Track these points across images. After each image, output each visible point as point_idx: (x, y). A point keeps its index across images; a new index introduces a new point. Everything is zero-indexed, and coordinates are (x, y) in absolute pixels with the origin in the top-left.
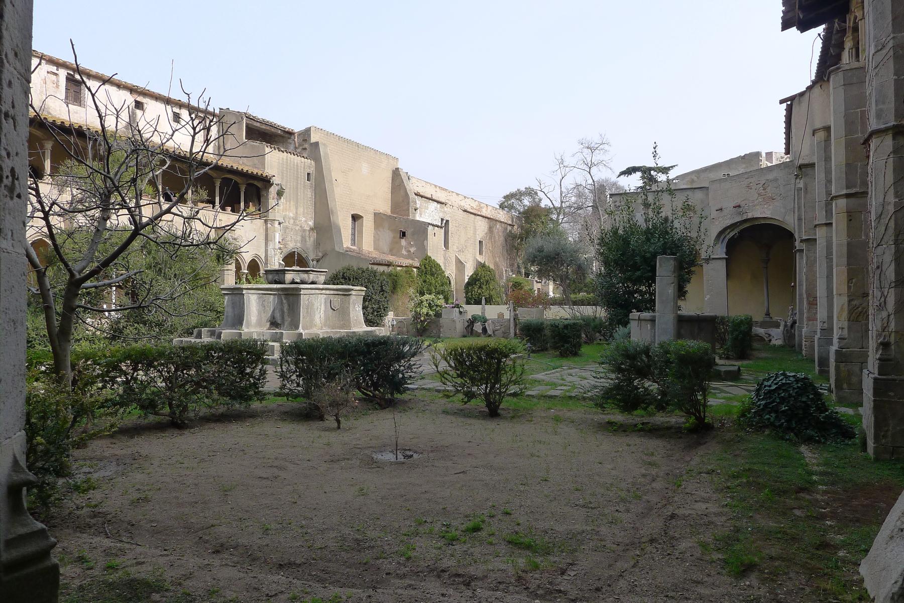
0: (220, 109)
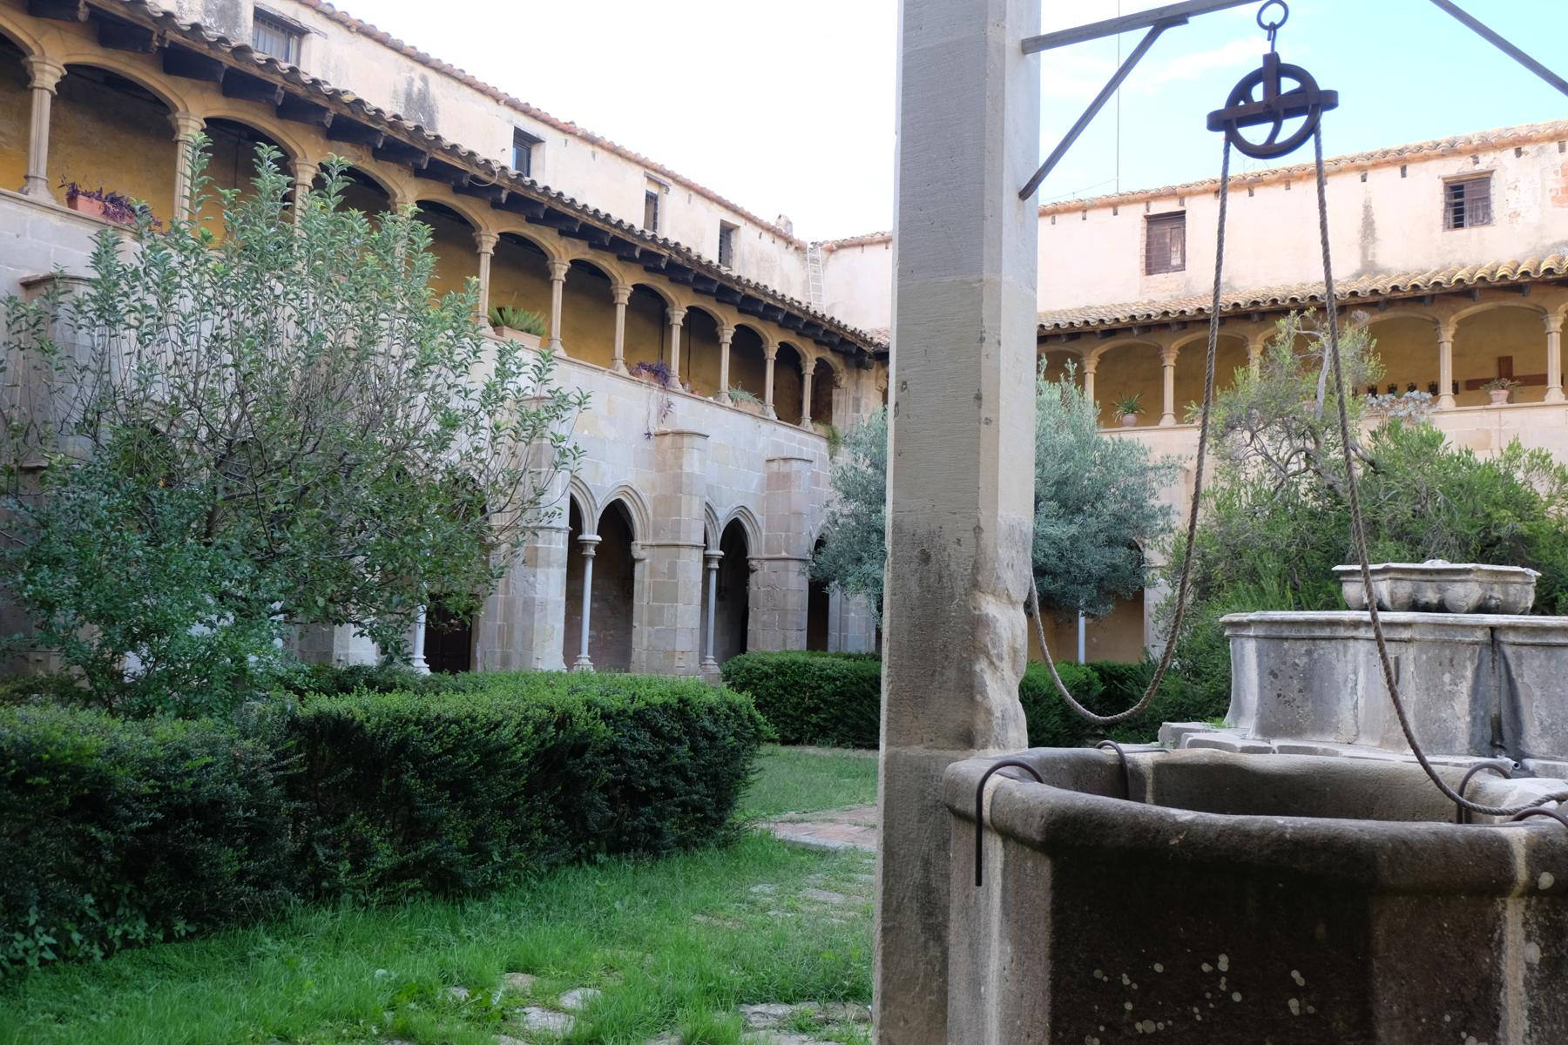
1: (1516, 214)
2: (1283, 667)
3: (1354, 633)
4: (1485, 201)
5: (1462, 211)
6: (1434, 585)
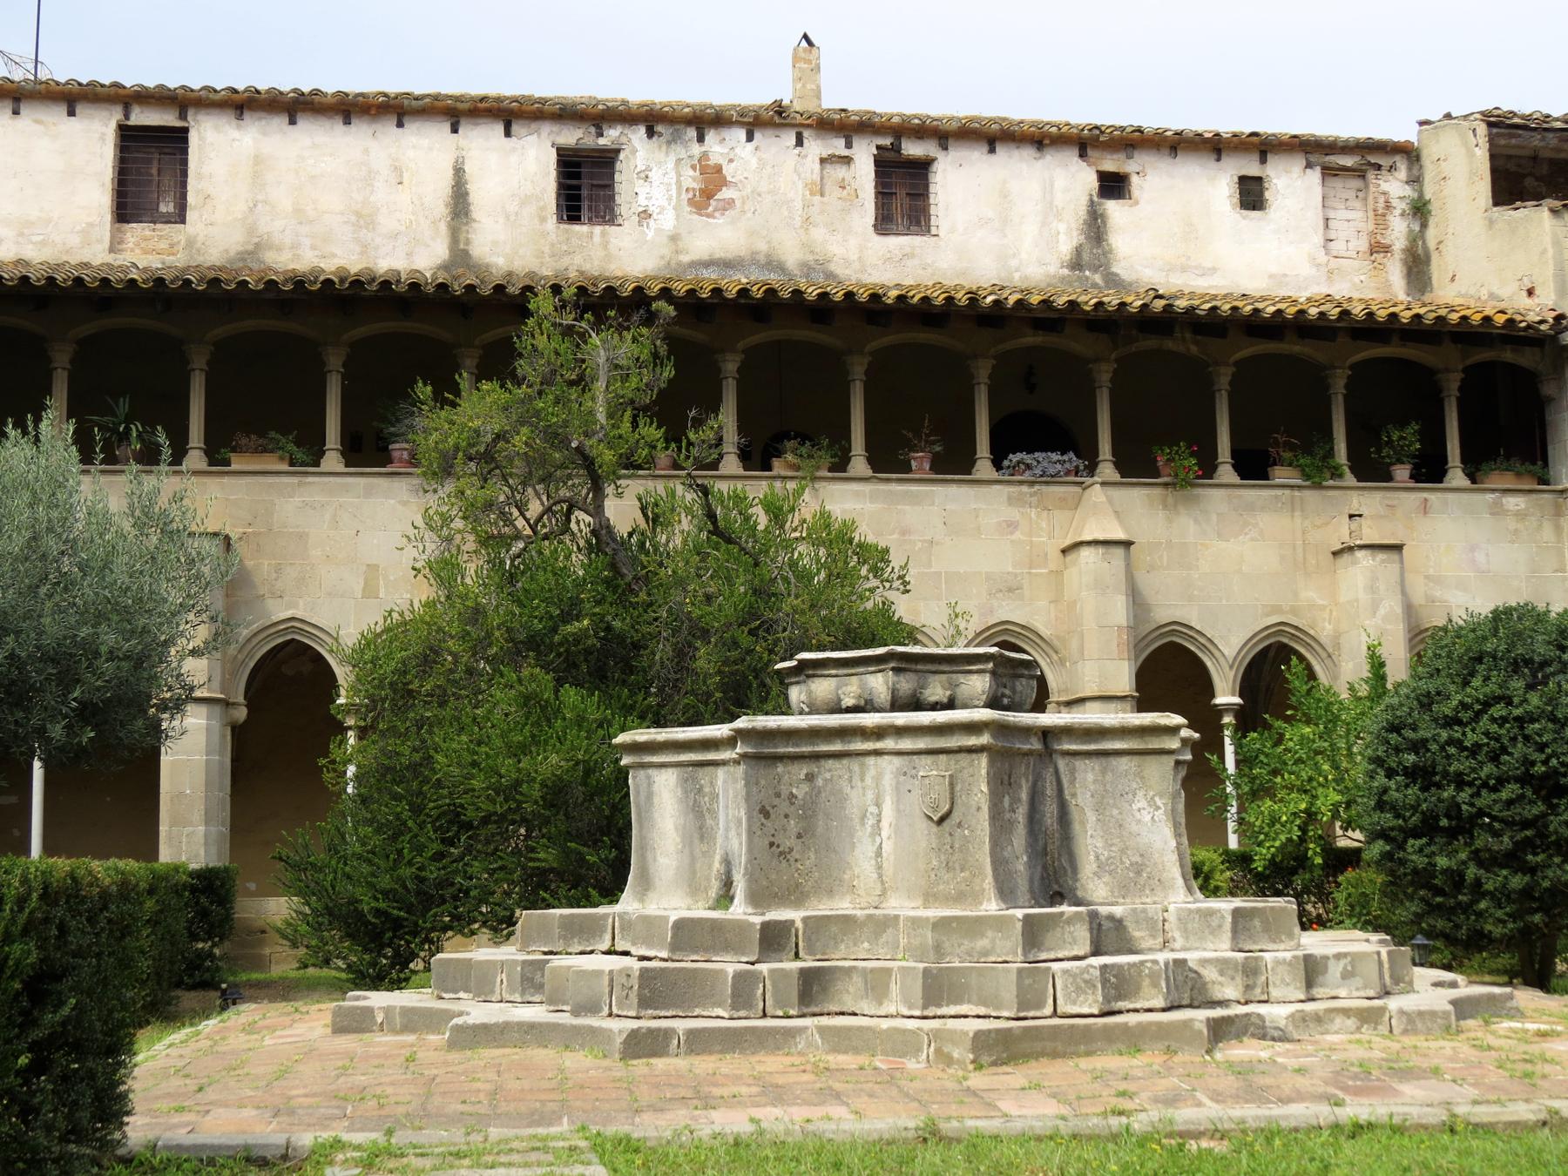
0: (1422, 123)
1: (645, 215)
2: (776, 801)
3: (879, 745)
4: (606, 190)
5: (578, 198)
6: (944, 677)
